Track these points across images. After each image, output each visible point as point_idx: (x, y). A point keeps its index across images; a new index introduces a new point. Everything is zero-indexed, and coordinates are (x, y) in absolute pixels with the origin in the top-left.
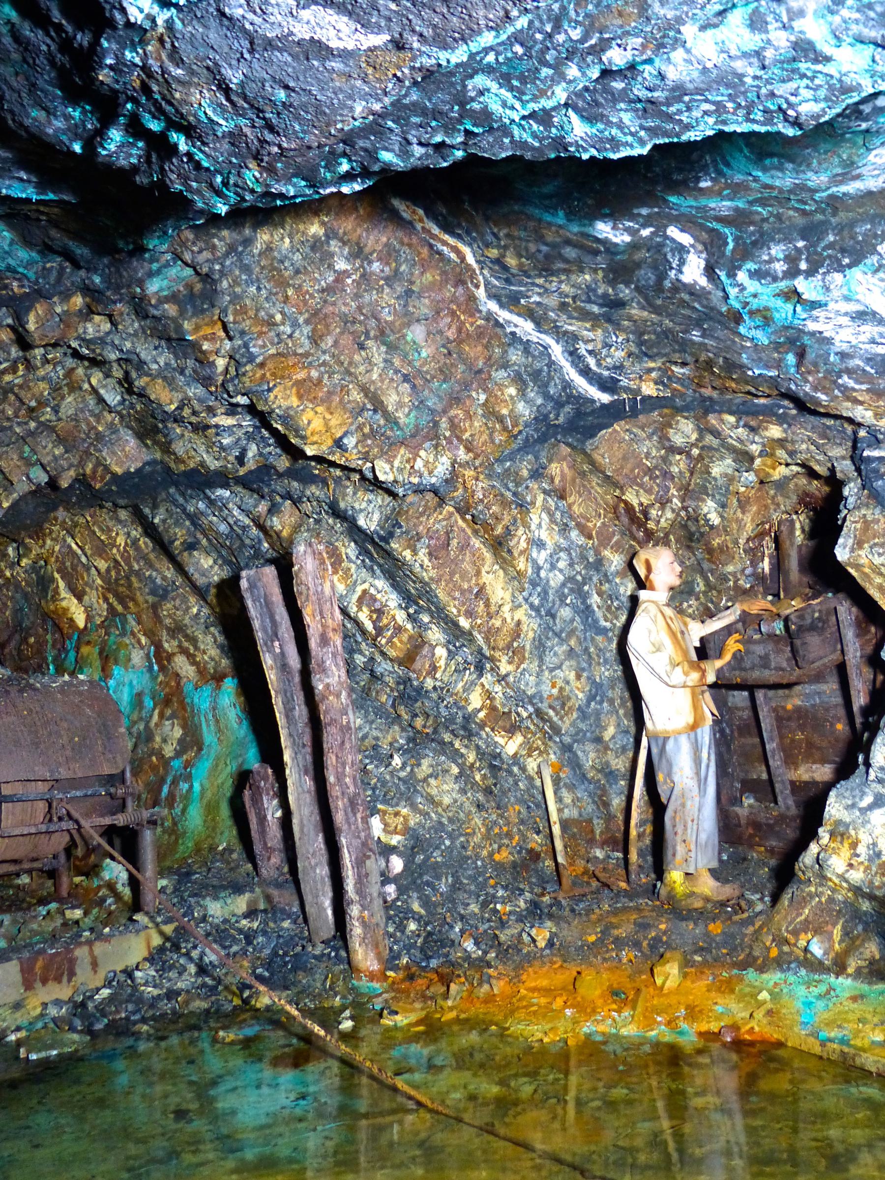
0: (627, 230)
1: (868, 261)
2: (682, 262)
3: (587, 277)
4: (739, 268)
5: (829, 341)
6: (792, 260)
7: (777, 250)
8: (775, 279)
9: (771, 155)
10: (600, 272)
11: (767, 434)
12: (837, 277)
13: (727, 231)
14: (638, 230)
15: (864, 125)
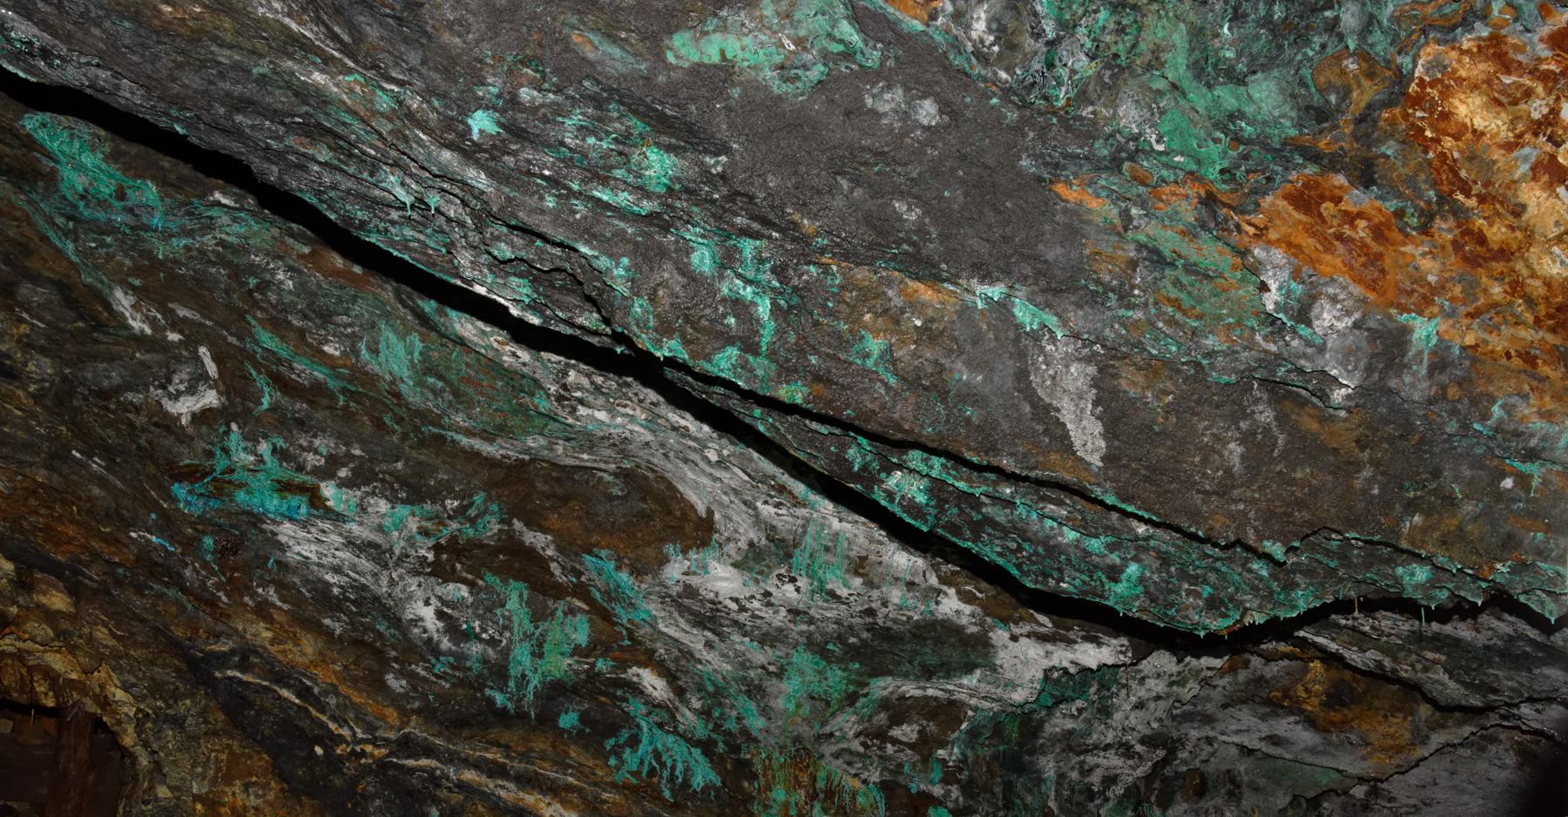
0: (152, 322)
1: (428, 506)
2: (192, 390)
4: (265, 437)
5: (283, 548)
6: (334, 462)
7: (324, 444)
9: (441, 378)
10: (24, 329)
11: (44, 600)
12: (383, 506)
13: (266, 389)
14: (165, 329)
15: (570, 421)
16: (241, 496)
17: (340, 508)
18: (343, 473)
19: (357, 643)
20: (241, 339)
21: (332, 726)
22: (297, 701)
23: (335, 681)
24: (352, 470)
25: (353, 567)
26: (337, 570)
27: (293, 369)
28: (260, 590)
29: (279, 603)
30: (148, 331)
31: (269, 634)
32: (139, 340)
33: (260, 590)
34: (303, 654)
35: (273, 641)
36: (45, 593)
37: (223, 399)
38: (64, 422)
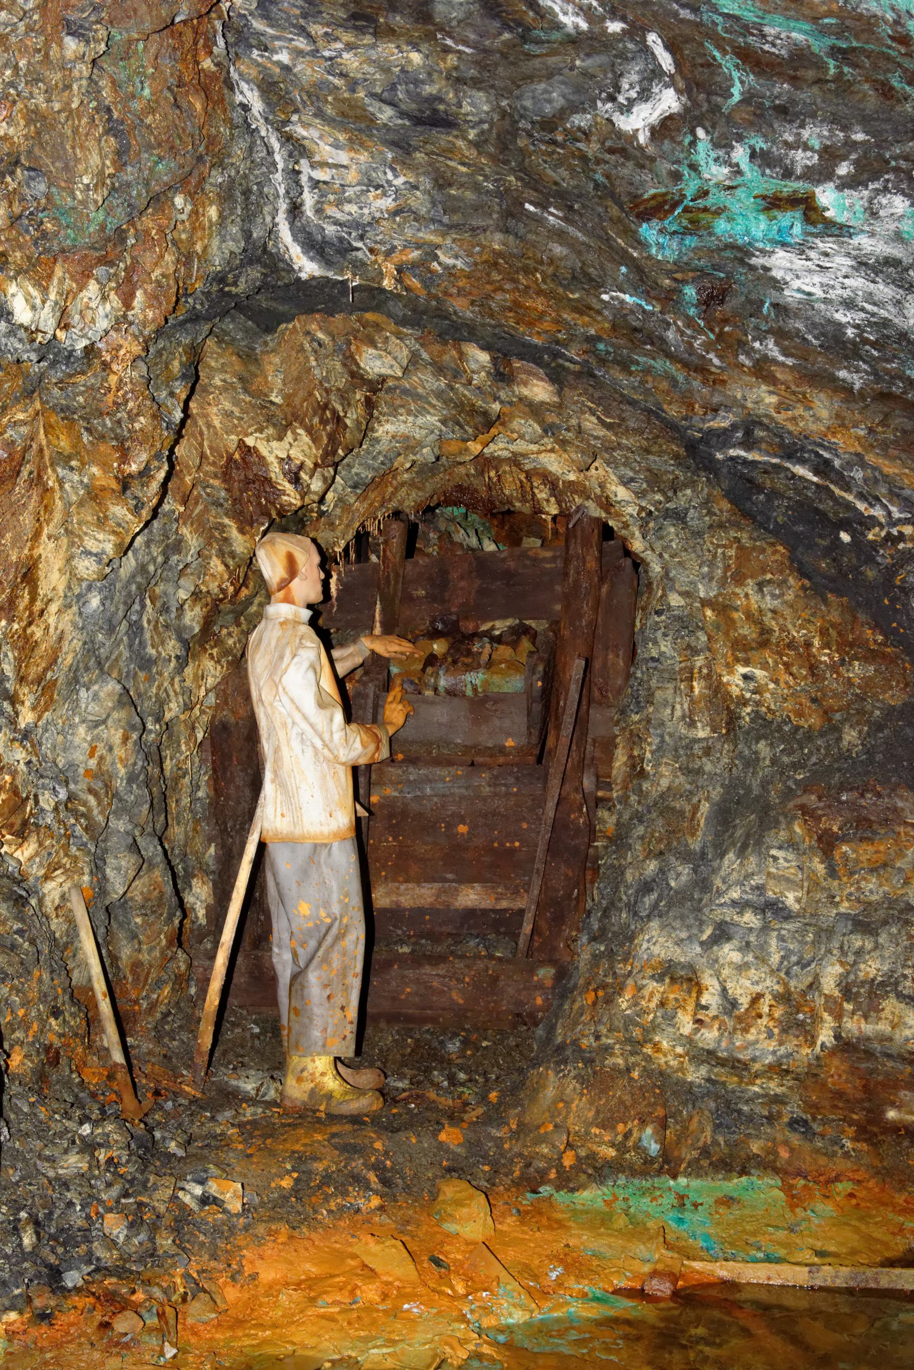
2: (645, 95)
3: (416, 58)
4: (740, 138)
5: (778, 285)
8: (788, 174)
10: (452, 60)
11: (525, 392)
13: (736, 74)
14: (603, 19)
16: (721, 226)
17: (841, 219)
18: (843, 169)
19: (884, 397)
20: (695, 10)
21: (861, 506)
22: (815, 479)
23: (860, 450)
24: (856, 163)
25: (870, 297)
26: (849, 304)
27: (764, 36)
28: (757, 345)
29: (781, 358)
30: (584, 26)
31: (773, 399)
32: (575, 41)
33: (757, 345)
34: (818, 419)
35: (778, 408)
36: (525, 384)
37: (684, 99)
38: (512, 171)
